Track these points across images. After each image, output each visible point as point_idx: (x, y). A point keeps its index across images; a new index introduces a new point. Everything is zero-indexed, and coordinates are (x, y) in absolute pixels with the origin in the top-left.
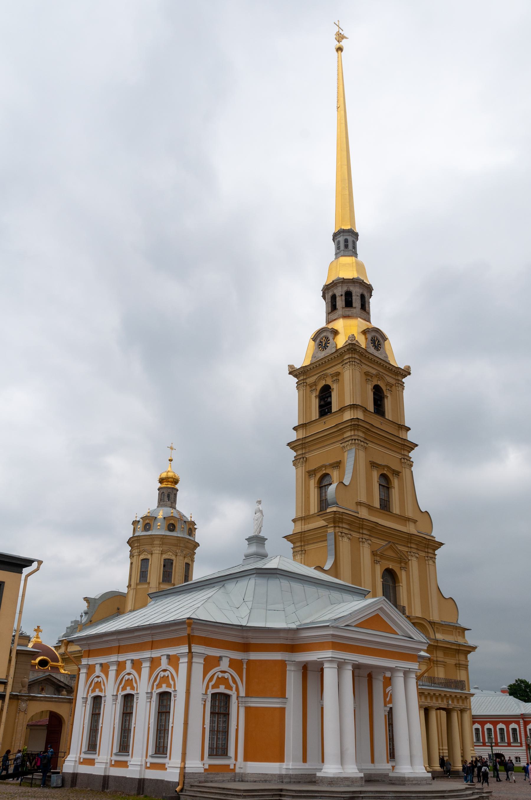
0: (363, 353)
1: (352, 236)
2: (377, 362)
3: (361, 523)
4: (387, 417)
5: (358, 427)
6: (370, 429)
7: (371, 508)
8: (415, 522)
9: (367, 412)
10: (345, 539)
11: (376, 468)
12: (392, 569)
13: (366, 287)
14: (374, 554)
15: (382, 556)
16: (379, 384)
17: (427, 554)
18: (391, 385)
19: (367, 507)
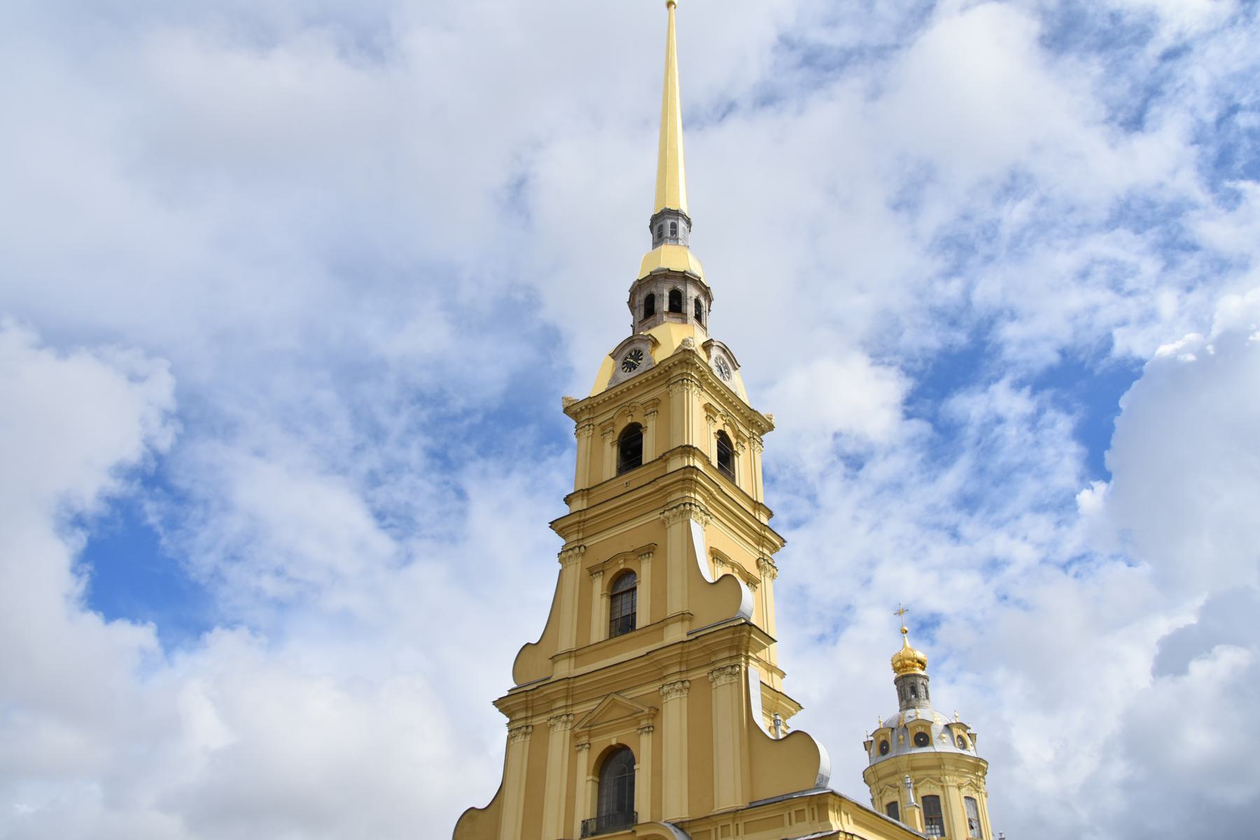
0: (589, 404)
1: (656, 223)
2: (622, 392)
3: (541, 695)
4: (643, 463)
5: (564, 533)
6: (582, 518)
7: (578, 653)
8: (684, 617)
9: (591, 491)
10: (520, 739)
11: (597, 574)
12: (619, 744)
13: (652, 279)
14: (575, 736)
15: (589, 731)
16: (629, 420)
17: (712, 668)
18: (656, 402)
19: (570, 657)
